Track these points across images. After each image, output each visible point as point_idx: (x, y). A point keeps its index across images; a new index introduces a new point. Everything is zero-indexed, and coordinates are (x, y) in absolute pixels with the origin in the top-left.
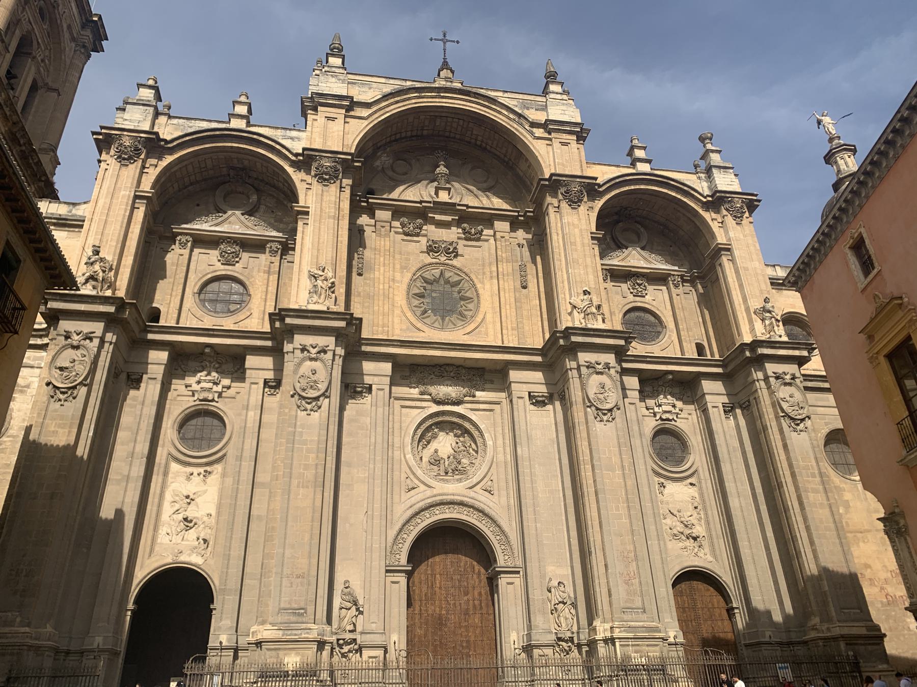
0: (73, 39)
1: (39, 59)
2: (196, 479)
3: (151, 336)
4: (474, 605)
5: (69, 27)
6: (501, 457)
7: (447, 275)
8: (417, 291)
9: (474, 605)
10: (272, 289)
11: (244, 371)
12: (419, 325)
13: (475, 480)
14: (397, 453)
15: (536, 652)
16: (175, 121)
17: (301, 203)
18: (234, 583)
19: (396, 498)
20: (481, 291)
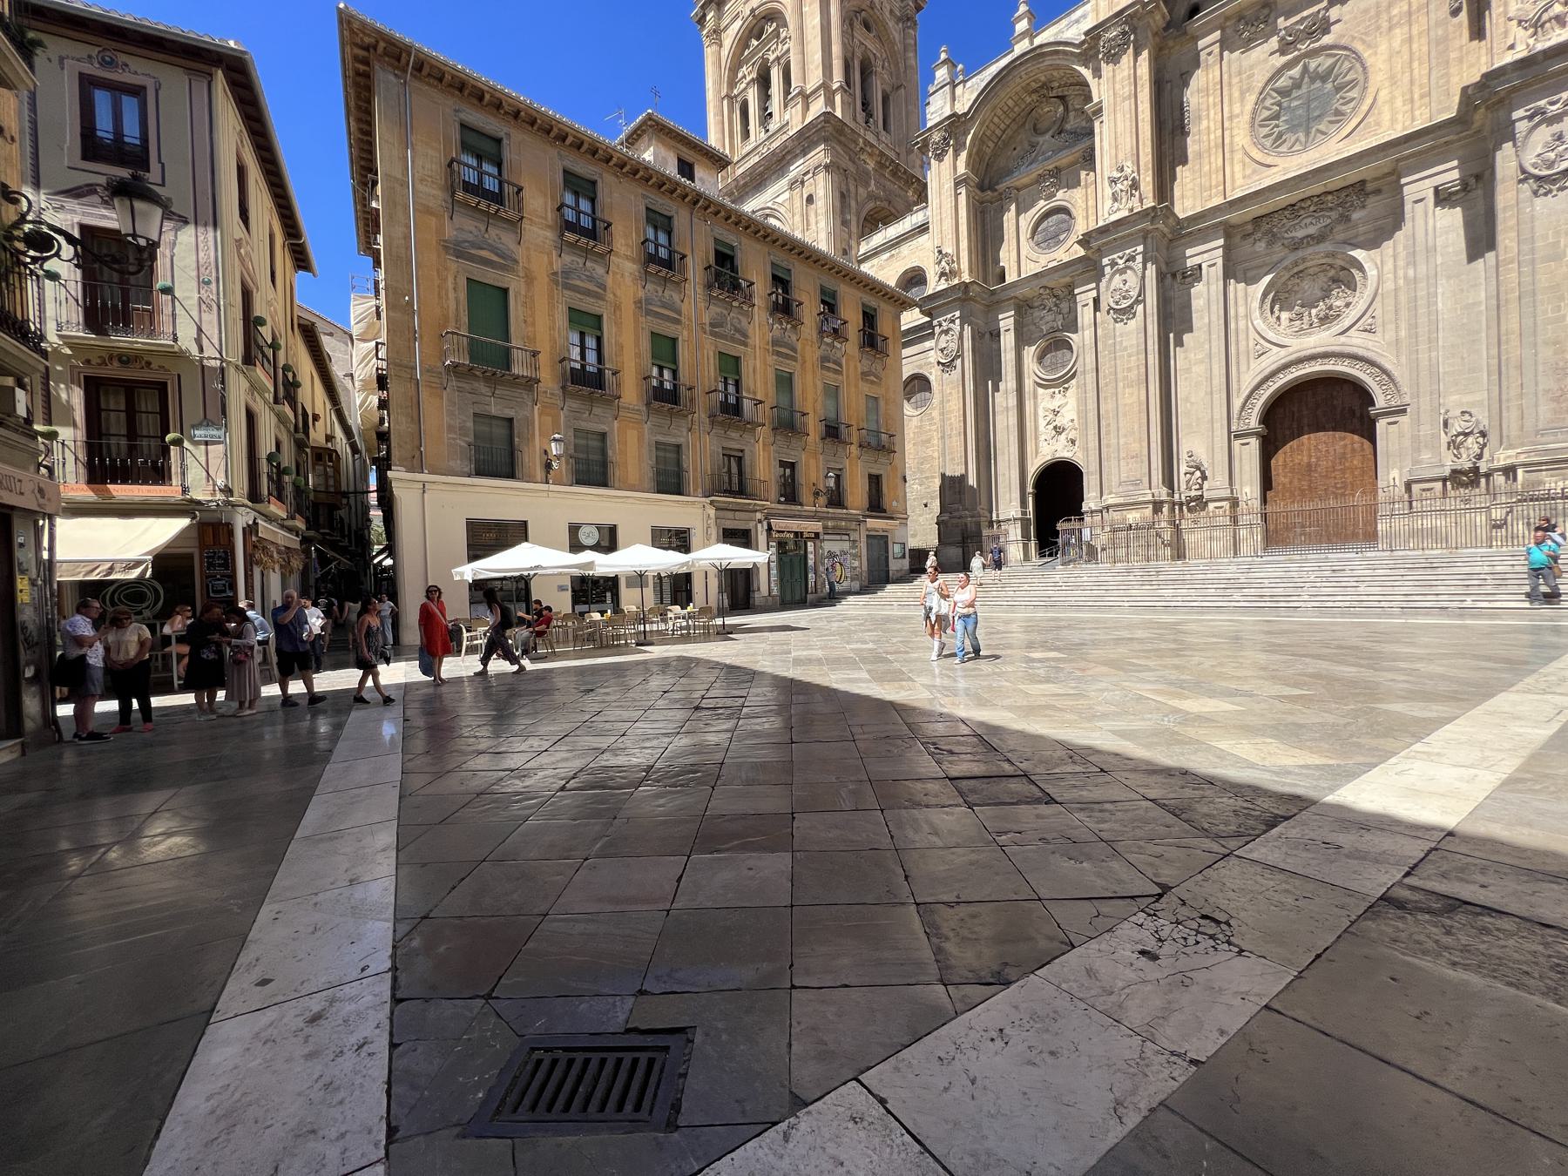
0: (899, 20)
1: (879, 69)
2: (1058, 396)
3: (996, 298)
4: (1353, 450)
5: (891, 11)
6: (1389, 285)
7: (1313, 65)
8: (1266, 113)
9: (1353, 450)
10: (1091, 203)
11: (1075, 296)
12: (1269, 161)
13: (1347, 323)
14: (1242, 324)
15: (1416, 488)
16: (969, 84)
17: (1096, 100)
18: (1094, 466)
19: (1243, 368)
20: (1369, 62)
